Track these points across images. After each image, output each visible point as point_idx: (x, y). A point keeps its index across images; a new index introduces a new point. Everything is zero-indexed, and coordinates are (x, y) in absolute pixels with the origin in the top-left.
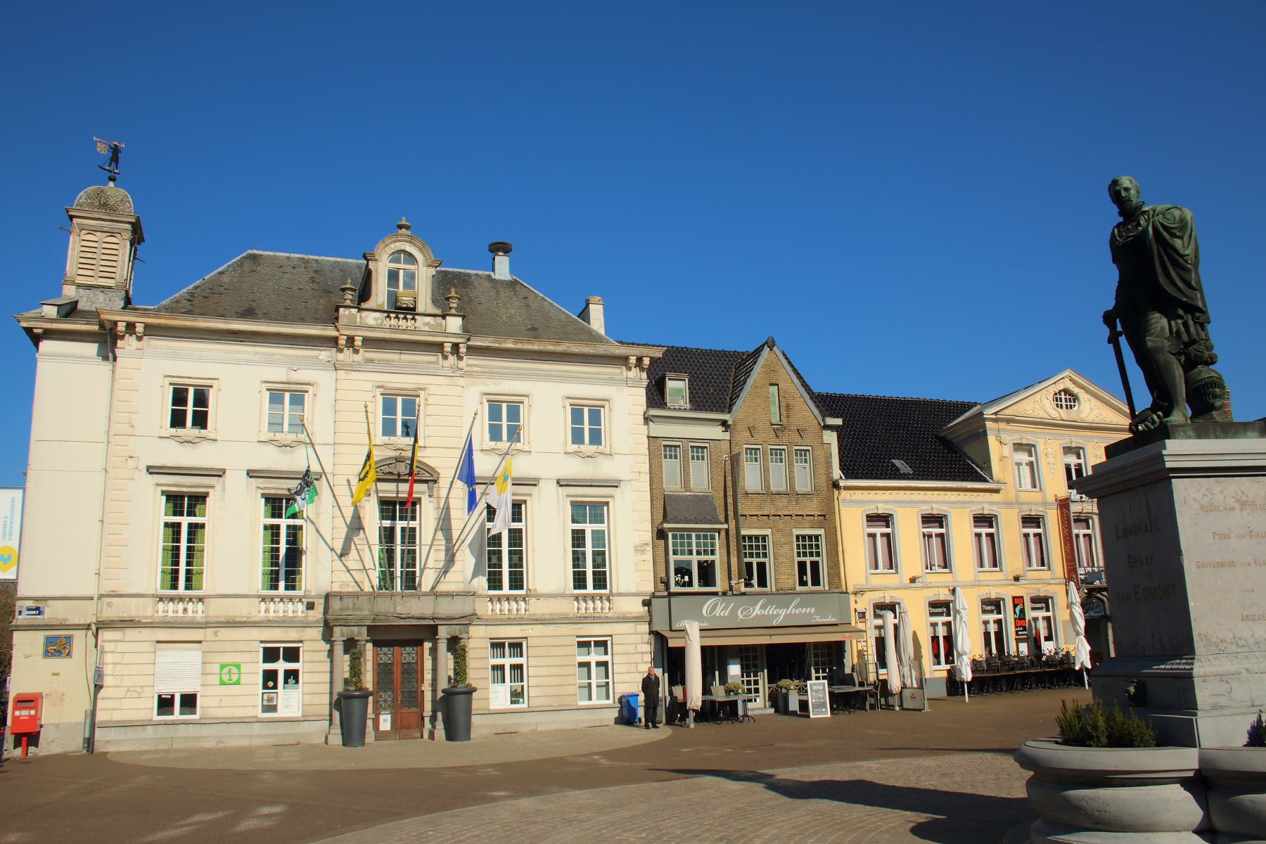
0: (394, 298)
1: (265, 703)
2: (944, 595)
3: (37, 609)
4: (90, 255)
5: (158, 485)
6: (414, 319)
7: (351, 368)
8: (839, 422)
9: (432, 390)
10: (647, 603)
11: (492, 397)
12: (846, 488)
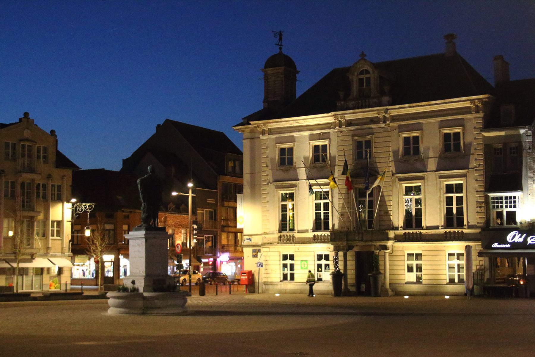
1: (318, 277)
3: (249, 239)
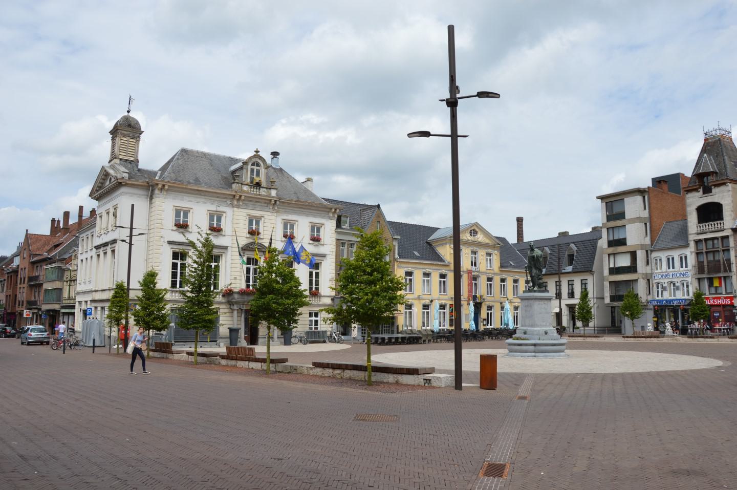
0: (252, 179)
2: (427, 302)
4: (124, 146)
5: (171, 248)
6: (259, 189)
7: (239, 207)
8: (399, 237)
9: (266, 217)
10: (333, 300)
11: (286, 221)
12: (399, 262)
